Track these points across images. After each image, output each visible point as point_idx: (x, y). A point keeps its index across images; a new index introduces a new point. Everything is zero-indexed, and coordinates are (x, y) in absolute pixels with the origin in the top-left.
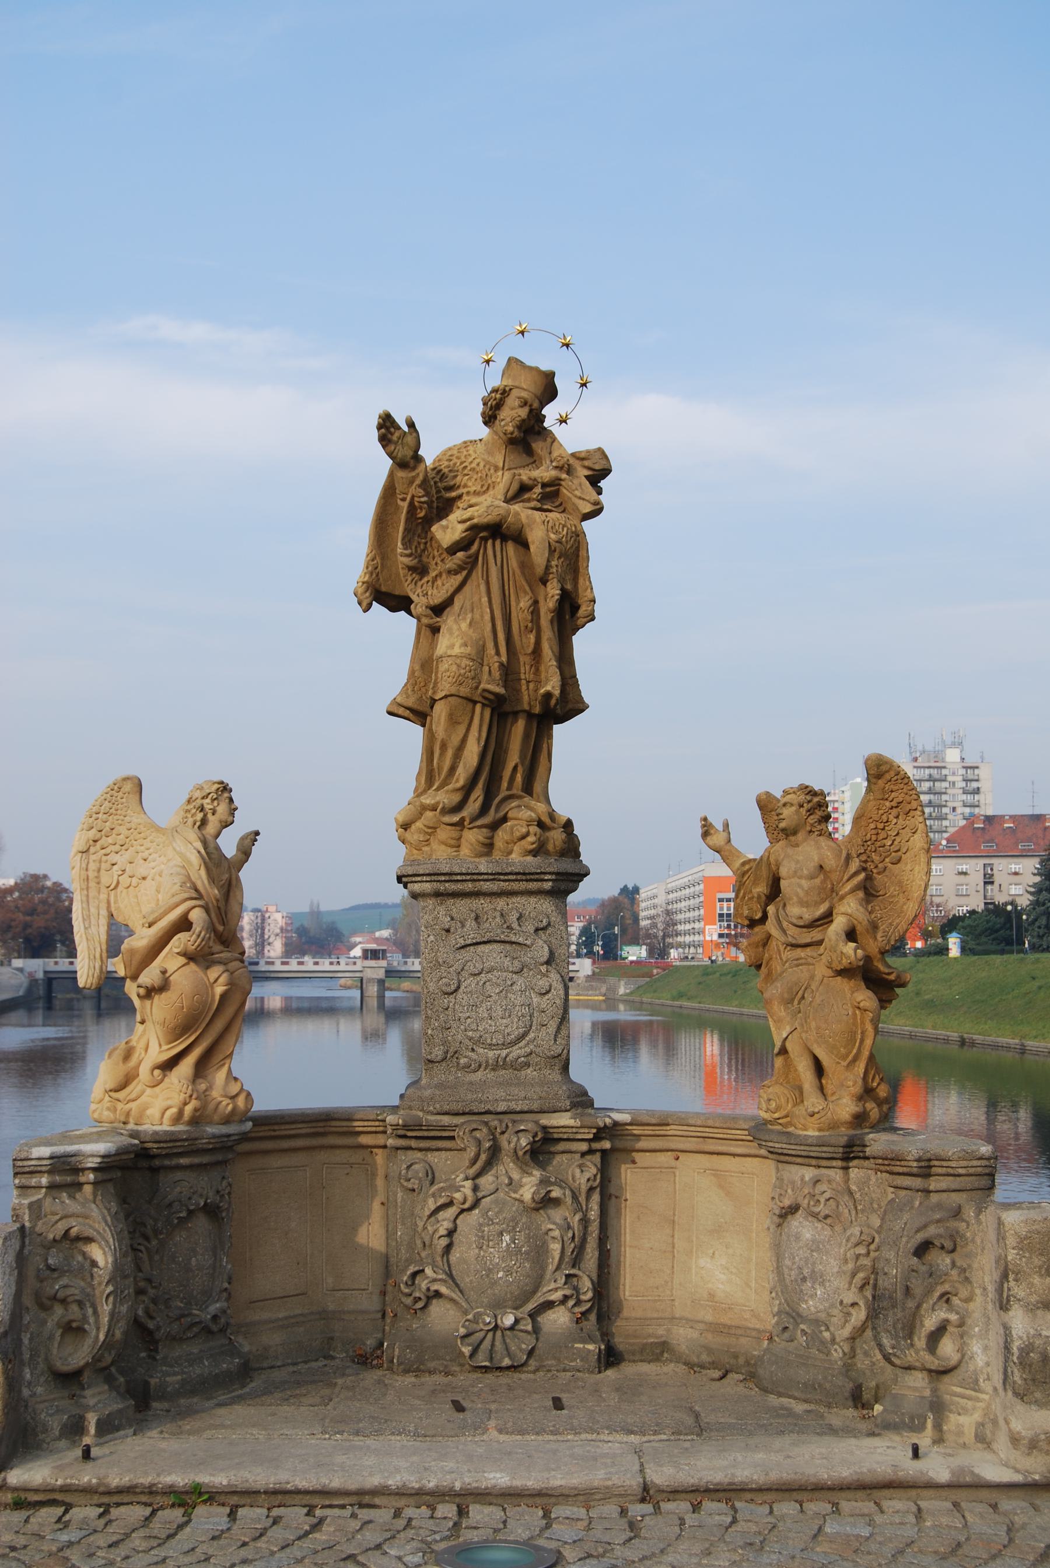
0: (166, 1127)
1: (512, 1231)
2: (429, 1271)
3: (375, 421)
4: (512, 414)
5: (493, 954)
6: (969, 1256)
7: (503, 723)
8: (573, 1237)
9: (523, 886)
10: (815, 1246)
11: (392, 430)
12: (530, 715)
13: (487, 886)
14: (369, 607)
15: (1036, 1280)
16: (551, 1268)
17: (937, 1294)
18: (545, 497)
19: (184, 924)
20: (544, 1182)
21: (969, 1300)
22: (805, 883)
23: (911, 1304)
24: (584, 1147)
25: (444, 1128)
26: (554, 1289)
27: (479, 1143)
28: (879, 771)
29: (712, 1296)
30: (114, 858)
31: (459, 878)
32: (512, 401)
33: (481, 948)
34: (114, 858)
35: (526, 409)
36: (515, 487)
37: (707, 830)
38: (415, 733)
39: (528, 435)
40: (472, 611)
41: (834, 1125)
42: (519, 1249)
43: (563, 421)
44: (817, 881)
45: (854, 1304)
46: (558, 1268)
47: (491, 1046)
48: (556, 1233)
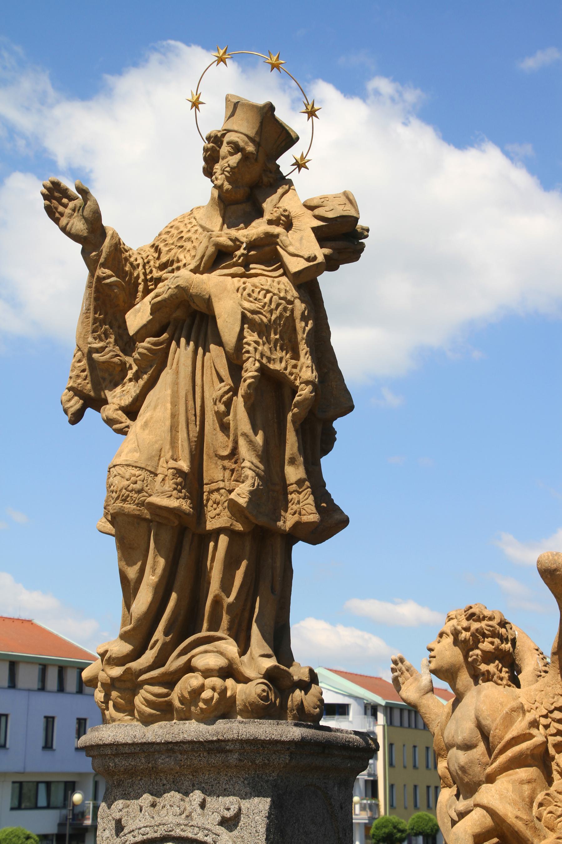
11: (65, 201)
14: (76, 417)
31: (126, 750)
32: (225, 149)
35: (239, 156)
36: (211, 249)
40: (155, 408)
43: (300, 165)
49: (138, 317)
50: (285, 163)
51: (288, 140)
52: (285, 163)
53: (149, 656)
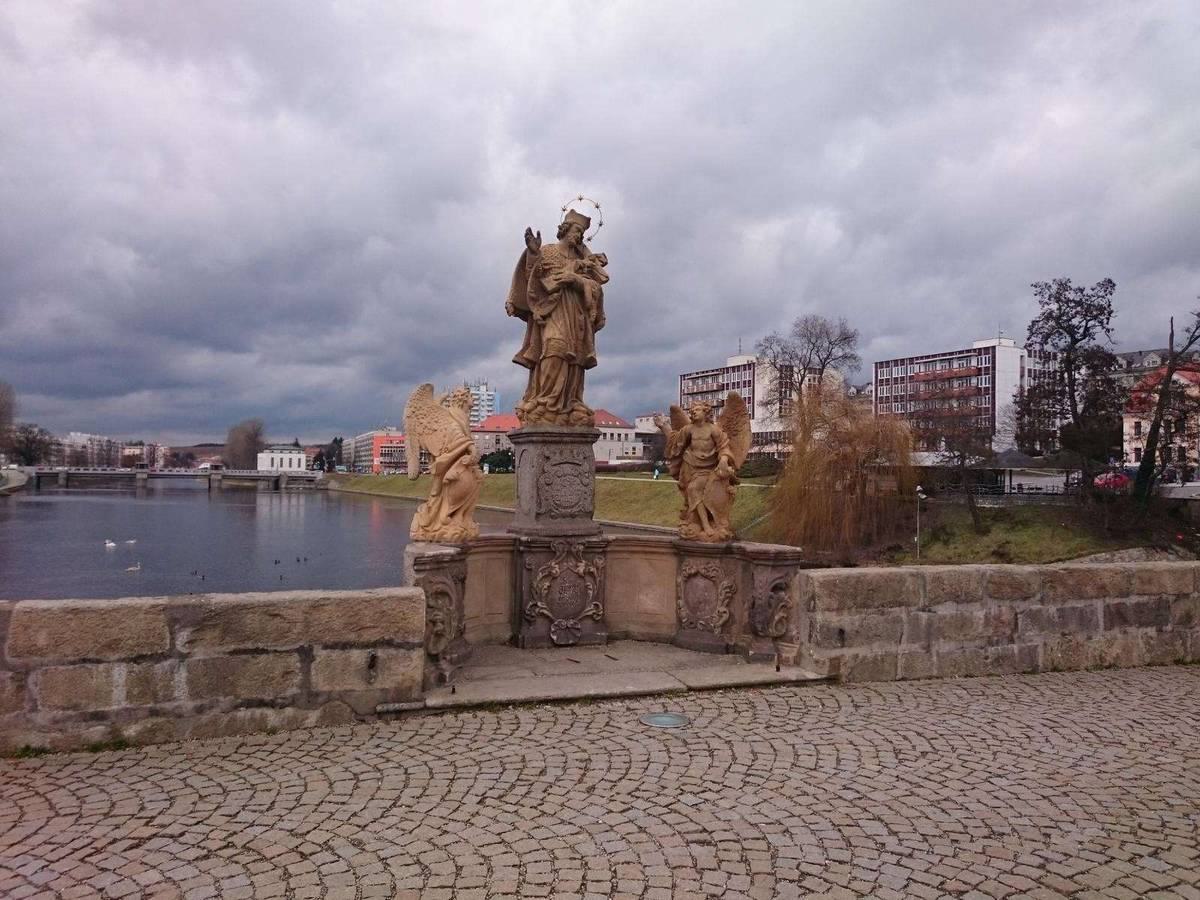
5: (567, 468)
7: (560, 370)
10: (706, 589)
12: (580, 366)
15: (825, 599)
22: (706, 442)
23: (771, 611)
25: (546, 542)
30: (422, 421)
32: (573, 228)
34: (422, 421)
39: (576, 248)
41: (722, 540)
43: (589, 240)
45: (725, 612)
47: (565, 508)
49: (550, 283)
53: (560, 406)
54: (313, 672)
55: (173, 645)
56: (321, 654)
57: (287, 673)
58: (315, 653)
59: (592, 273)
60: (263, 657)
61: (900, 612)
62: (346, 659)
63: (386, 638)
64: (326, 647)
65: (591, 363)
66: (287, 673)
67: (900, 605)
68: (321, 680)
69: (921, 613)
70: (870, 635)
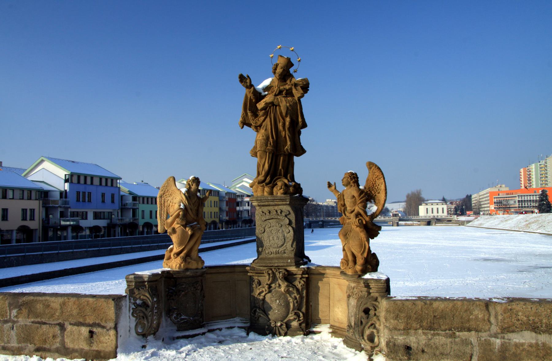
0: (177, 270)
1: (279, 299)
2: (258, 310)
3: (238, 76)
4: (279, 70)
6: (379, 312)
7: (280, 157)
8: (297, 302)
9: (281, 203)
13: (271, 203)
14: (242, 127)
15: (392, 321)
16: (291, 310)
17: (369, 324)
18: (286, 94)
19: (178, 216)
20: (287, 286)
21: (380, 325)
23: (362, 327)
24: (300, 276)
25: (261, 270)
26: (291, 316)
27: (269, 274)
28: (371, 165)
29: (338, 319)
33: (270, 221)
37: (330, 185)
38: (256, 160)
42: (281, 305)
44: (353, 200)
46: (293, 310)
48: (291, 300)
50: (291, 70)
51: (292, 65)
52: (291, 70)
54: (66, 337)
55: (10, 316)
56: (69, 328)
57: (54, 337)
58: (65, 326)
59: (289, 93)
60: (44, 327)
61: (472, 337)
62: (80, 331)
63: (97, 322)
64: (71, 324)
65: (299, 150)
66: (54, 337)
67: (469, 330)
68: (68, 341)
69: (493, 339)
70: (438, 353)
